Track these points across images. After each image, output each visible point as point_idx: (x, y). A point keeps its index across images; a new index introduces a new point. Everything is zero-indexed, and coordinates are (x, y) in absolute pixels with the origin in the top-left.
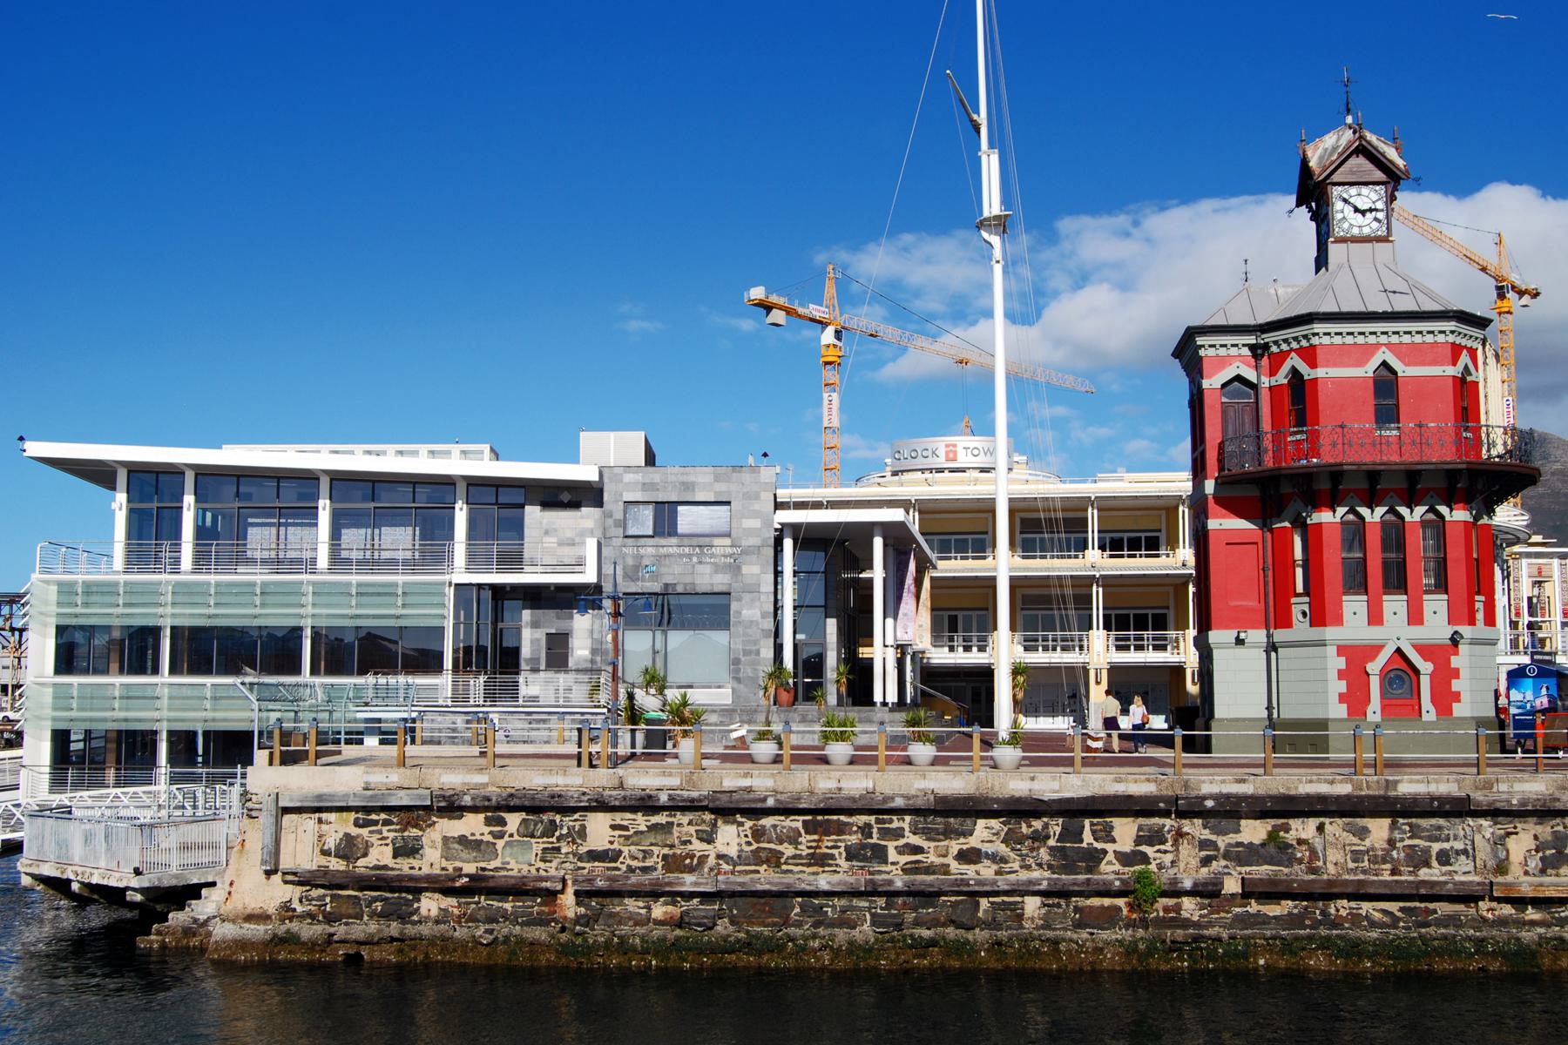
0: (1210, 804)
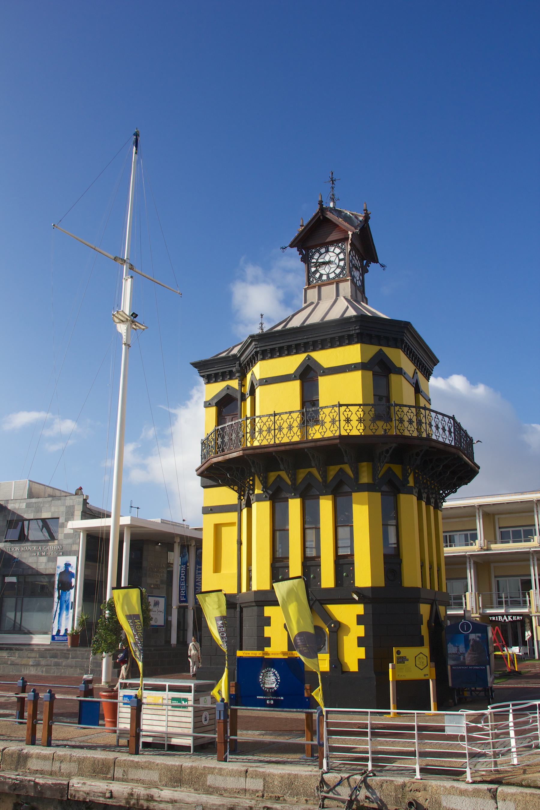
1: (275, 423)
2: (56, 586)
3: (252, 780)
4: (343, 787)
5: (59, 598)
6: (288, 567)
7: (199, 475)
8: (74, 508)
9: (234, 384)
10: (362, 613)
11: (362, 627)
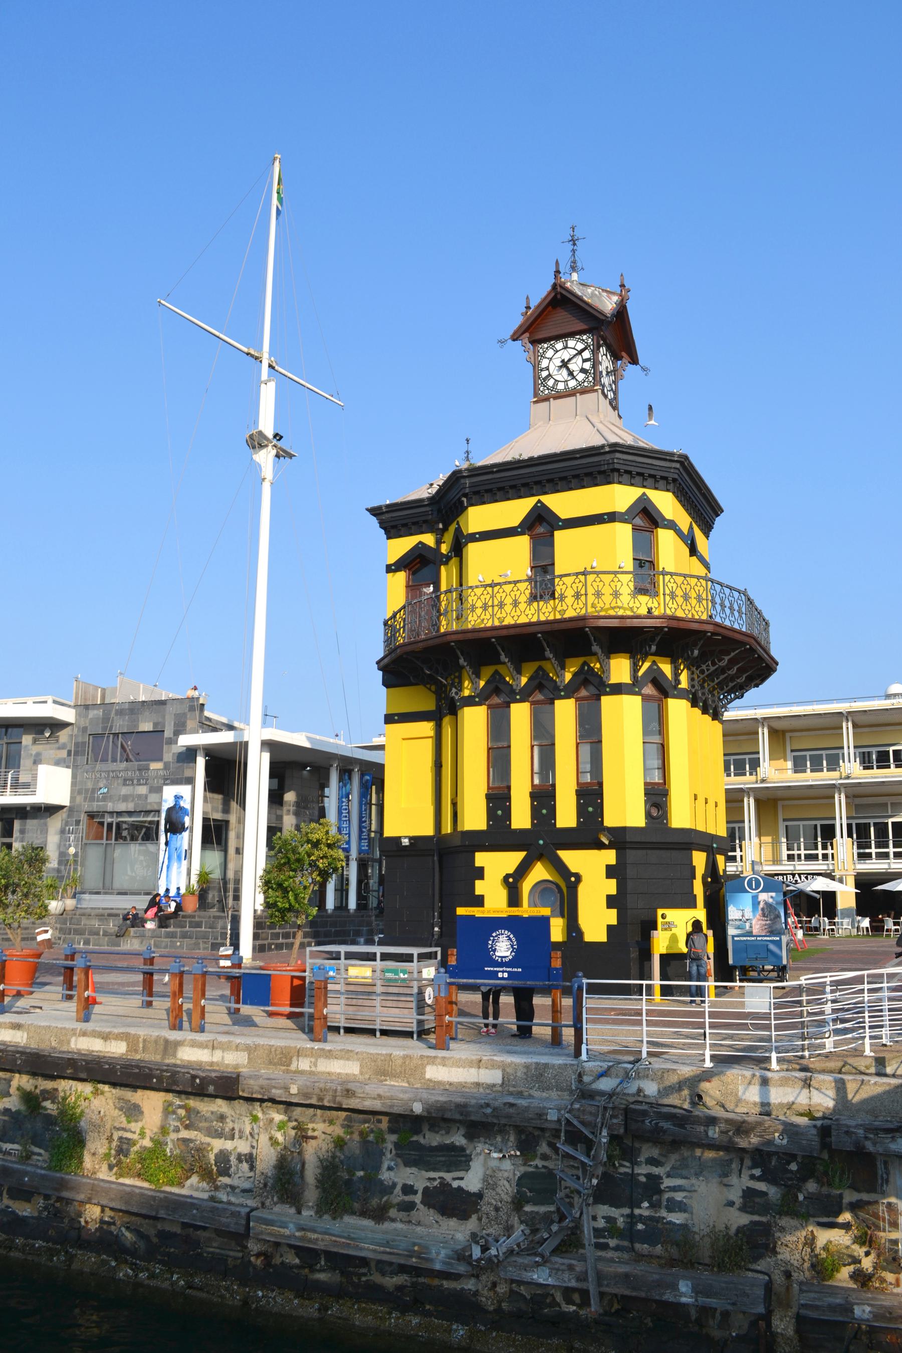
1: (493, 597)
2: (162, 827)
3: (487, 1071)
4: (609, 1078)
5: (167, 844)
6: (510, 798)
7: (379, 669)
8: (186, 717)
9: (429, 539)
10: (612, 861)
11: (614, 881)
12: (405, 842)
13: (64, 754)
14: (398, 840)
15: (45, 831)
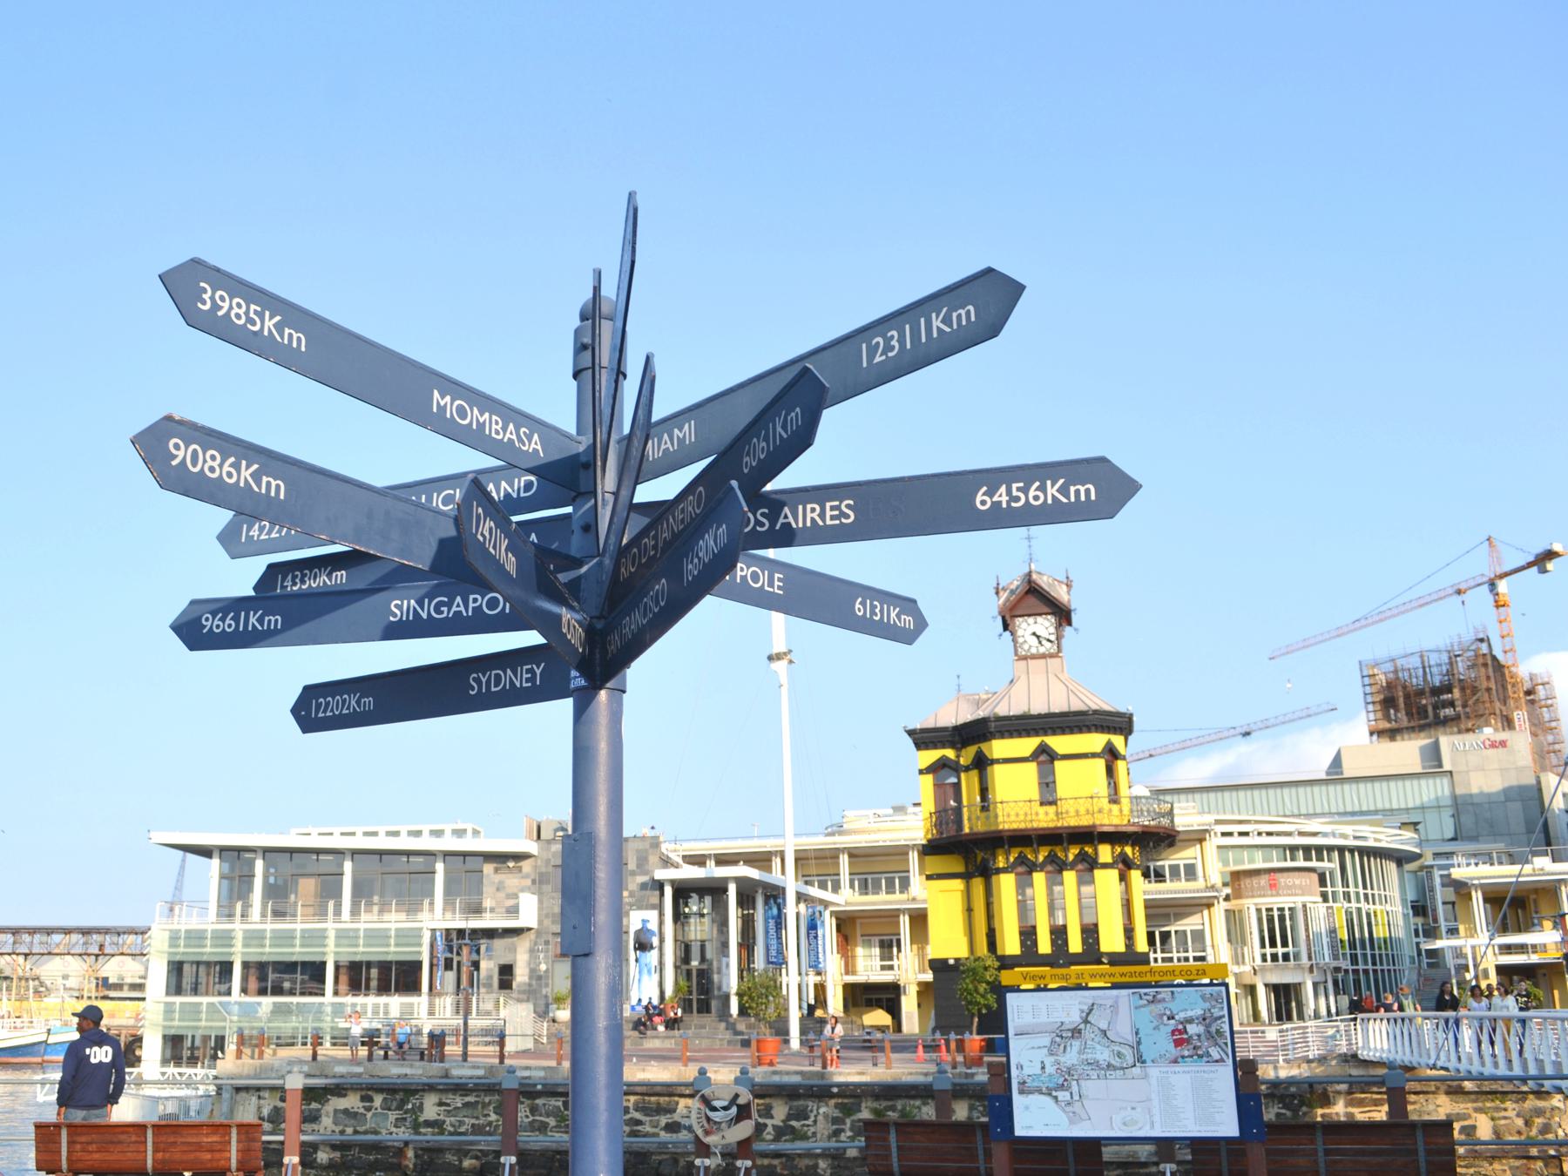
0: (835, 1090)
9: (950, 753)
12: (951, 962)
13: (528, 882)
14: (945, 961)
15: (513, 950)
